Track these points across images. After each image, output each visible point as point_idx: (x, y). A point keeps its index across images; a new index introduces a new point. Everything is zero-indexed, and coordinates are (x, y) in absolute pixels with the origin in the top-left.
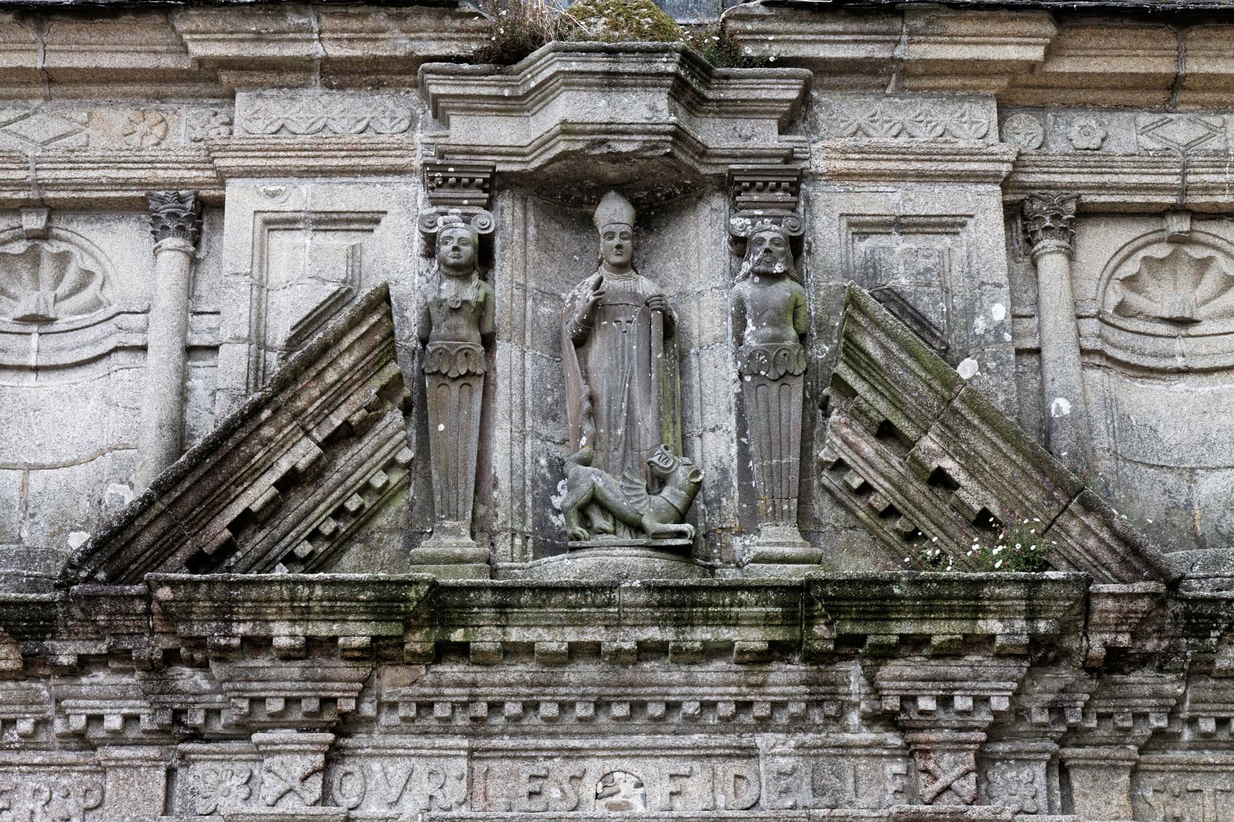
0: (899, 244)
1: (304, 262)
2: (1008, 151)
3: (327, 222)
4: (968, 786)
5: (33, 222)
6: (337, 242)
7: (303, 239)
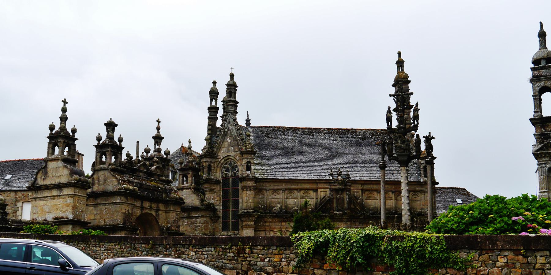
0: (356, 193)
3: (324, 191)
4: (358, 225)
5: (307, 190)
6: (325, 193)
7: (323, 193)
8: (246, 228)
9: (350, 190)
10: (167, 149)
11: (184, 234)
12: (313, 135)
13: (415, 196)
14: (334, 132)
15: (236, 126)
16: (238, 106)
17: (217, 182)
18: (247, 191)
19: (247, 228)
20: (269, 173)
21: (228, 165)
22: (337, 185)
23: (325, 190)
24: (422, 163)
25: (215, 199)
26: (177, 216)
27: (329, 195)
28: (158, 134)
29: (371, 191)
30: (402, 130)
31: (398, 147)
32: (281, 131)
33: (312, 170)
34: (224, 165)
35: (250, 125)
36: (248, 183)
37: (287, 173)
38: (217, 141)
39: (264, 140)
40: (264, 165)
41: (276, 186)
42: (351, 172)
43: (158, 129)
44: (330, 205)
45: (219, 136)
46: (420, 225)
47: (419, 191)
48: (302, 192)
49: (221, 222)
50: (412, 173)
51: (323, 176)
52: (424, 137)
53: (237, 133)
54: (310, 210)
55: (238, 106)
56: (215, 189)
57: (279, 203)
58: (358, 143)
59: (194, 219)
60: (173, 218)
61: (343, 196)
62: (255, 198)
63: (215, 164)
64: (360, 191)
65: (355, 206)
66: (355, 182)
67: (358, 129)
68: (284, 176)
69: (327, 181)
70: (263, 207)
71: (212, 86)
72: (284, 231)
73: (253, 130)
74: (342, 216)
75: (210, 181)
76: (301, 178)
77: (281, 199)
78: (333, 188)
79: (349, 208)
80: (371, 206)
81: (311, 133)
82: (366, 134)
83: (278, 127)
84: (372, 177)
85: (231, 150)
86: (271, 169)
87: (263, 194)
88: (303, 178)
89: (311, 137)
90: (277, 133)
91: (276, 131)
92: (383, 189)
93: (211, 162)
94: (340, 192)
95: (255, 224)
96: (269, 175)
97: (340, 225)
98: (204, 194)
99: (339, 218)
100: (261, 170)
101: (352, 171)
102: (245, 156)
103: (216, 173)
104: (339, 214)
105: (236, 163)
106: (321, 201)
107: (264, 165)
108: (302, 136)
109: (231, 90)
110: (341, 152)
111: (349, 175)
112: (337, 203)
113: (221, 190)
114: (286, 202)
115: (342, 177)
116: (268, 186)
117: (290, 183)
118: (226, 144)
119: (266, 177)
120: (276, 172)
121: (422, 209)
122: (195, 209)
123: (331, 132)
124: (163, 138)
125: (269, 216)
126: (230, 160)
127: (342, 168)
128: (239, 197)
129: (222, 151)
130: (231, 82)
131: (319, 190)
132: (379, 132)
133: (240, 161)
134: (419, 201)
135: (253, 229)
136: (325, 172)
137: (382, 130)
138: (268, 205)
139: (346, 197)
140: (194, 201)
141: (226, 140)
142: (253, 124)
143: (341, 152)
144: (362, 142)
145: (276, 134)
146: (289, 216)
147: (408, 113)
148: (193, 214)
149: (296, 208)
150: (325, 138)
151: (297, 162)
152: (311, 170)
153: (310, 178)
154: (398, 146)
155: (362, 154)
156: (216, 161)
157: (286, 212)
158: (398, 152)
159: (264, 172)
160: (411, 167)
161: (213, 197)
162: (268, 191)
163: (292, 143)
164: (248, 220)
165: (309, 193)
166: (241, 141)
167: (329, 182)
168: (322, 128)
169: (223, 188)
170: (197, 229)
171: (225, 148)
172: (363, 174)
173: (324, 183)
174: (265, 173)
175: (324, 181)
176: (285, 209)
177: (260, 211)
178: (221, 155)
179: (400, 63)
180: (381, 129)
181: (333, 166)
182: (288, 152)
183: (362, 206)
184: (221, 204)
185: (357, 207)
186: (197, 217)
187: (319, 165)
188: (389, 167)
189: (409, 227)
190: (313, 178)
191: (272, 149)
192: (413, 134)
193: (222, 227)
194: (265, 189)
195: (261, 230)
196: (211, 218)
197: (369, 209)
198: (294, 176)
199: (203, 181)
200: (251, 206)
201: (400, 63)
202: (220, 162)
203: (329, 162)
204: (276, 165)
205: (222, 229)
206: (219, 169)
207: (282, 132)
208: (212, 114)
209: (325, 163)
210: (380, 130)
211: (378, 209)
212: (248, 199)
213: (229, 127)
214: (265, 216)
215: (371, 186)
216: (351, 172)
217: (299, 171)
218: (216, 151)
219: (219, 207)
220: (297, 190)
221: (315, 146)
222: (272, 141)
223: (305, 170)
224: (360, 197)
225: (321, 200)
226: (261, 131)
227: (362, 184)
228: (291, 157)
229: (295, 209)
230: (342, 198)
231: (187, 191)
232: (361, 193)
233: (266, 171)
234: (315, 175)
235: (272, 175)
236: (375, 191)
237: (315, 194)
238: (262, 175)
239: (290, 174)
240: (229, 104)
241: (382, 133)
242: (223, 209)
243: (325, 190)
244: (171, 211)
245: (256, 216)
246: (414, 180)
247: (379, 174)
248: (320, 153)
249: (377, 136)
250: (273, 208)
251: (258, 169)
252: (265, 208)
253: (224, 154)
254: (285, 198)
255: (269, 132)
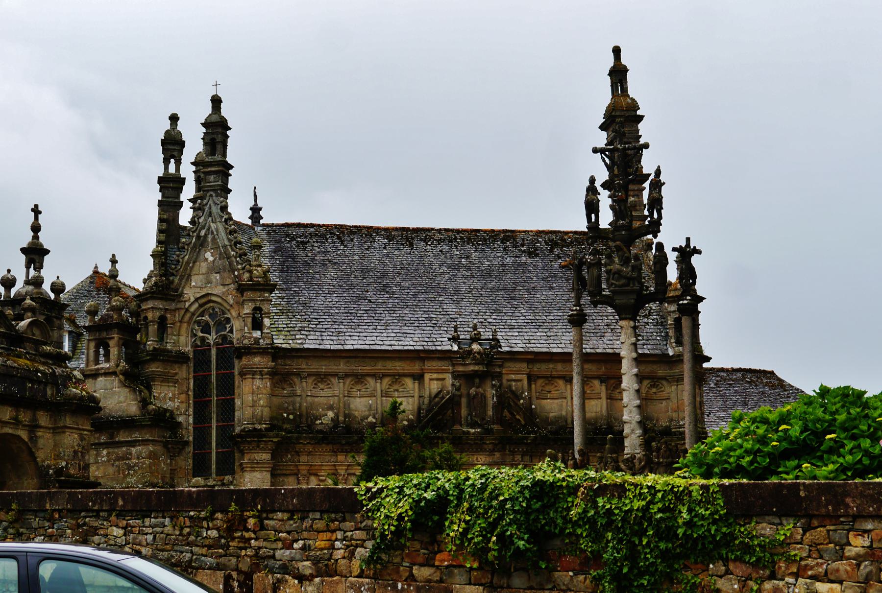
0: (514, 383)
1: (436, 386)
2: (528, 370)
3: (438, 379)
5: (397, 377)
6: (440, 382)
7: (435, 382)
8: (252, 468)
9: (499, 376)
10: (58, 277)
11: (100, 484)
12: (411, 245)
13: (654, 390)
14: (462, 238)
15: (227, 224)
16: (231, 175)
17: (180, 358)
18: (253, 378)
19: (253, 469)
20: (307, 335)
21: (206, 318)
22: (470, 364)
23: (441, 376)
24: (670, 312)
25: (176, 400)
26: (81, 441)
27: (450, 388)
28: (35, 241)
29: (550, 379)
30: (623, 233)
31: (615, 273)
32: (335, 234)
33: (410, 328)
34: (198, 317)
35: (262, 222)
36: (257, 359)
37: (350, 336)
38: (181, 260)
39: (294, 258)
40: (294, 316)
41: (323, 367)
42: (503, 334)
43: (36, 228)
44: (453, 412)
45: (186, 247)
46: (668, 458)
47: (664, 378)
48: (386, 381)
49: (191, 454)
50: (648, 334)
51: (436, 343)
52: (674, 249)
53: (230, 240)
54: (406, 423)
55: (231, 175)
56: (176, 374)
57: (331, 408)
58: (520, 265)
59: (124, 449)
60: (73, 447)
61: (485, 391)
62: (272, 395)
63: (175, 316)
64: (525, 378)
65: (512, 414)
66: (513, 356)
67: (520, 232)
68: (343, 342)
69: (445, 355)
70: (291, 417)
71: (169, 128)
72: (344, 475)
73: (268, 234)
74: (482, 439)
75: (163, 356)
76: (383, 348)
77: (336, 398)
78: (459, 371)
79: (499, 419)
80: (551, 415)
81: (407, 239)
82: (539, 242)
83: (328, 226)
84: (552, 345)
85: (214, 280)
86: (310, 326)
87: (291, 385)
88: (389, 348)
89: (407, 249)
90: (327, 239)
91: (323, 236)
92: (578, 373)
93: (166, 310)
94: (477, 380)
95: (273, 458)
96: (308, 341)
97: (477, 459)
98: (149, 388)
99: (475, 443)
100: (286, 329)
101: (505, 330)
102: (249, 294)
103: (179, 335)
104: (474, 434)
105: (227, 312)
106: (430, 401)
107: (294, 316)
108: (385, 248)
109: (213, 136)
110: (479, 285)
111: (498, 340)
112: (469, 405)
113: (191, 376)
114: (347, 406)
115: (480, 344)
116: (304, 366)
117: (357, 360)
118: (203, 267)
119: (298, 346)
120: (323, 334)
121: (671, 420)
122: (127, 423)
123: (456, 239)
124: (47, 252)
125: (305, 438)
126: (212, 304)
127: (482, 322)
128: (233, 394)
129: (193, 284)
130: (215, 118)
131: (427, 377)
132: (569, 237)
133: (236, 307)
134: (664, 402)
135: (267, 471)
136: (441, 332)
137: (576, 233)
138: (304, 413)
139: (490, 393)
140: (124, 404)
141: (201, 257)
142: (267, 218)
143: (479, 285)
144: (529, 260)
145: (324, 243)
146: (356, 438)
147: (636, 193)
148: (122, 437)
149: (371, 419)
150: (441, 251)
151: (374, 310)
152: (407, 328)
153: (406, 348)
154: (613, 271)
155: (528, 290)
156: (179, 306)
157: (348, 430)
158: (612, 284)
159: (295, 333)
160: (646, 320)
161: (170, 395)
162: (305, 378)
163: (361, 263)
164: (255, 449)
165: (403, 384)
166: (238, 259)
167: (450, 358)
168: (433, 229)
169: (194, 372)
170: (132, 472)
171: (201, 276)
172: (531, 338)
173: (440, 359)
174: (297, 337)
175: (437, 356)
176: (344, 422)
177: (286, 426)
178: (190, 293)
179: (618, 74)
180: (574, 229)
181: (461, 320)
182: (352, 286)
183: (530, 414)
184: (191, 410)
185: (518, 417)
186: (133, 443)
187: (427, 316)
188: (593, 320)
189: (640, 463)
190: (412, 348)
191: (313, 278)
192: (649, 243)
193: (193, 467)
194: (298, 375)
195: (288, 472)
196: (165, 445)
197: (546, 421)
198: (367, 342)
199: (147, 355)
200: (262, 414)
201: (618, 74)
202: (187, 310)
203: (451, 308)
204: (324, 317)
205: (194, 472)
206: (185, 324)
207: (339, 238)
208: (170, 193)
209: (440, 312)
210: (571, 232)
211: (566, 421)
212: (255, 398)
213: (209, 227)
214: (298, 438)
215: (551, 366)
216: (503, 334)
217: (378, 331)
218: (179, 284)
219: (187, 419)
220: (373, 376)
221: (417, 270)
222: (313, 260)
223: (392, 327)
224: (523, 393)
225: (431, 399)
226: (288, 235)
227: (529, 362)
228: (359, 298)
229: (370, 422)
230: (482, 394)
231: (106, 380)
232: (525, 382)
233: (299, 331)
234: (417, 339)
235: (314, 342)
236: (560, 377)
237: (417, 385)
238: (291, 342)
239: (357, 338)
240: (209, 169)
241: (576, 240)
242: (194, 423)
243: (441, 376)
244: (66, 430)
245: (275, 440)
246: (652, 352)
247: (568, 338)
248: (429, 288)
249: (563, 246)
250: (317, 419)
251: (280, 326)
252: (298, 419)
253: (198, 290)
254: (345, 396)
255: (306, 238)
